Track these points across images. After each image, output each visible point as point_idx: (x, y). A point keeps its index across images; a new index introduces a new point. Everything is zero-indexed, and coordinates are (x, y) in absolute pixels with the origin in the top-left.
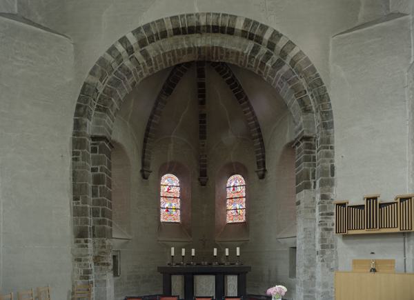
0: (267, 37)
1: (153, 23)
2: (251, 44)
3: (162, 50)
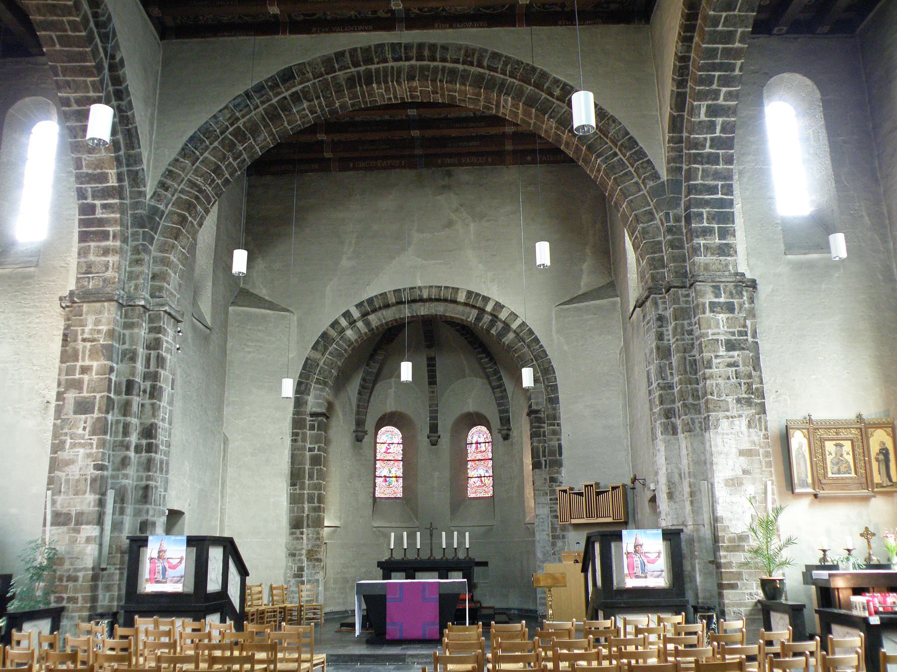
0: (489, 308)
1: (376, 296)
2: (475, 312)
3: (384, 318)
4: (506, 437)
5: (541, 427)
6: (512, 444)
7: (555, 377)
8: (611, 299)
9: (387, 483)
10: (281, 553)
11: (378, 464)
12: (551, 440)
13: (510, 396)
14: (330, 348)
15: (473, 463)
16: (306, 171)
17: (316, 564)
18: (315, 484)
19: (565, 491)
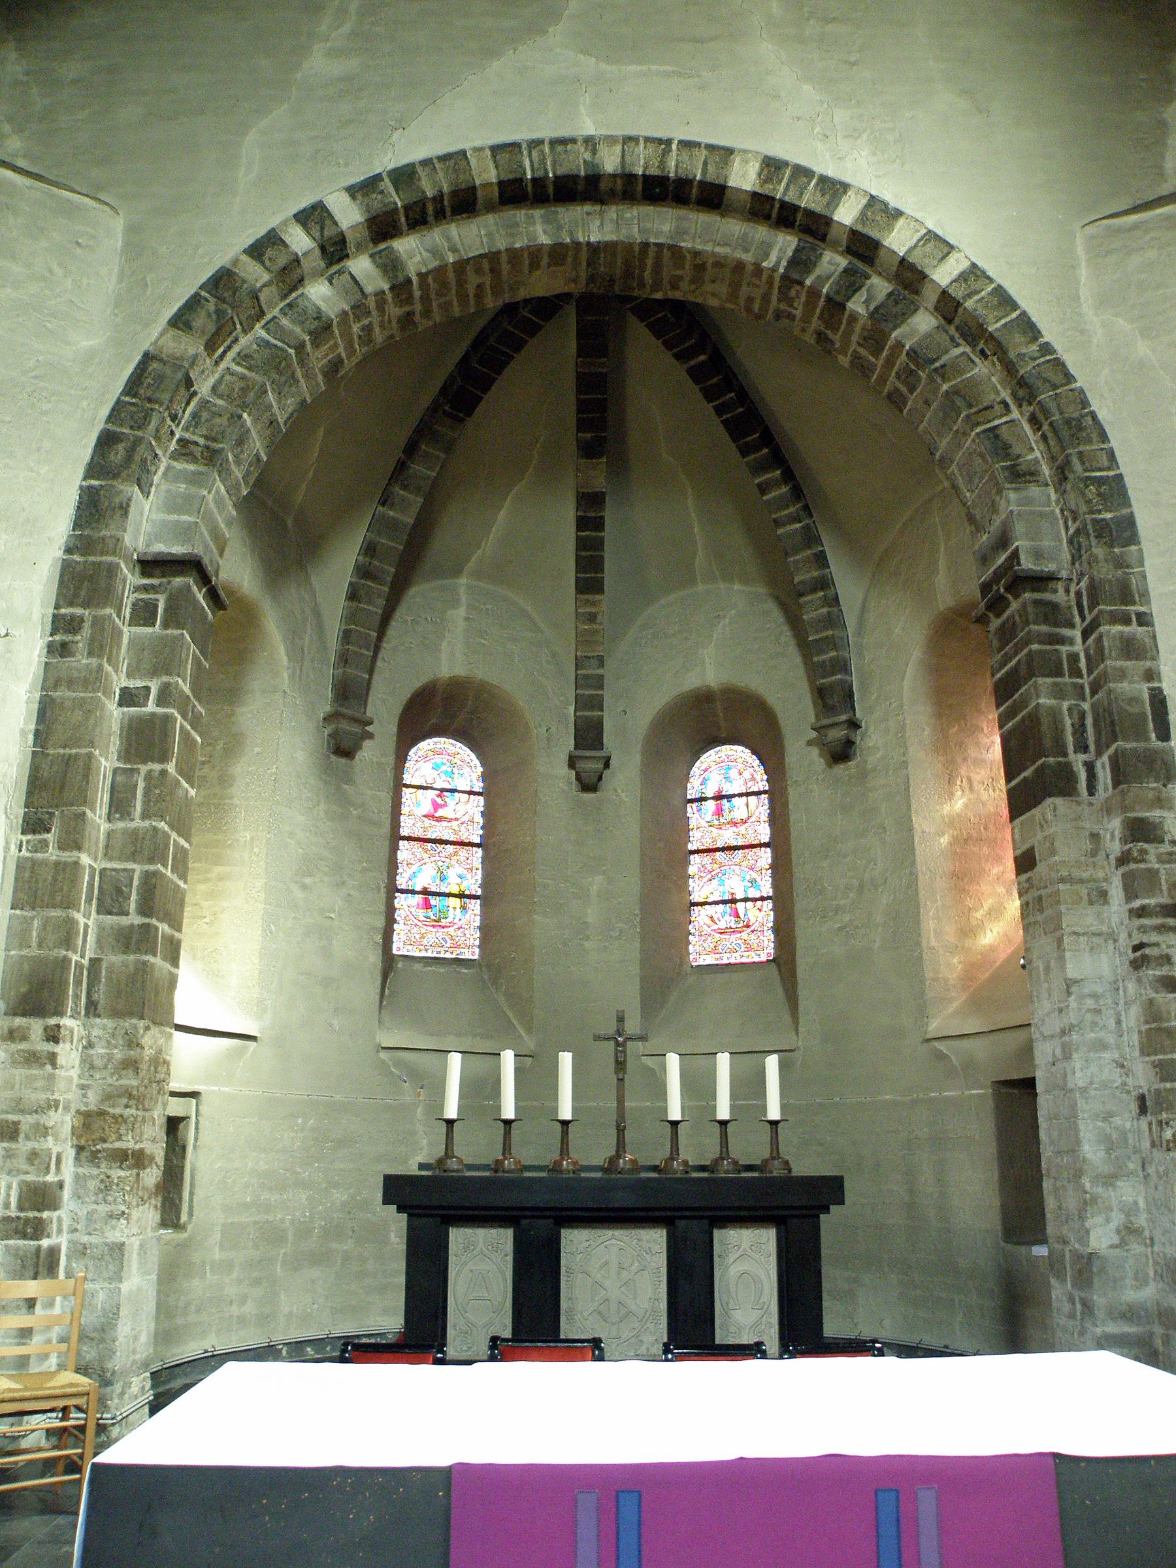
1: (426, 163)
3: (454, 250)
5: (1062, 640)
6: (863, 775)
7: (1111, 455)
11: (405, 851)
12: (1122, 675)
13: (851, 622)
14: (244, 341)
15: (706, 859)
17: (117, 1173)
18: (134, 835)
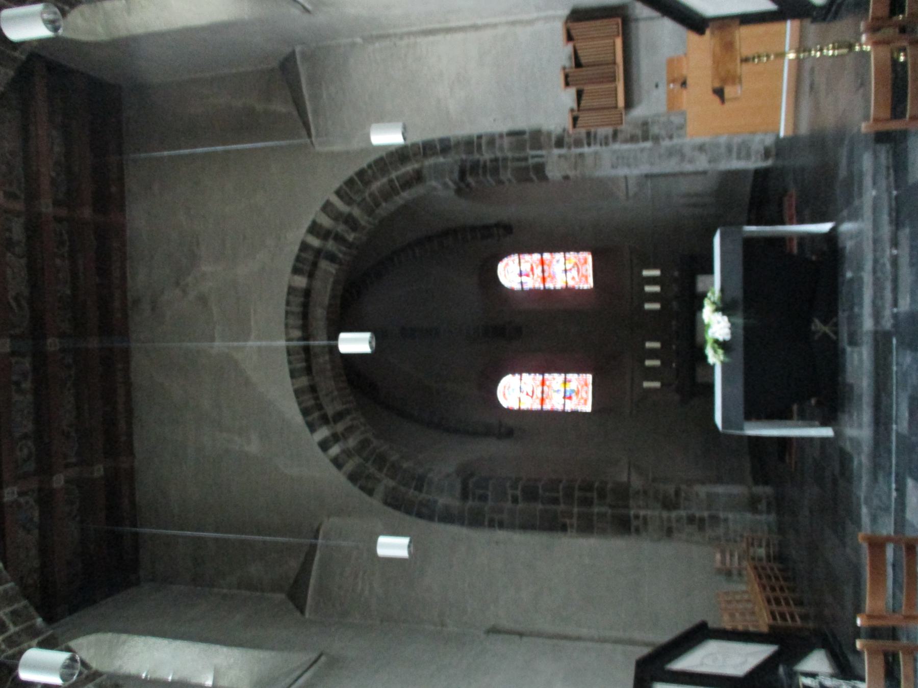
0: (315, 242)
1: (300, 404)
2: (324, 264)
4: (508, 228)
8: (299, 62)
9: (574, 395)
10: (667, 549)
12: (501, 149)
16: (133, 503)
17: (683, 495)
19: (575, 120)
